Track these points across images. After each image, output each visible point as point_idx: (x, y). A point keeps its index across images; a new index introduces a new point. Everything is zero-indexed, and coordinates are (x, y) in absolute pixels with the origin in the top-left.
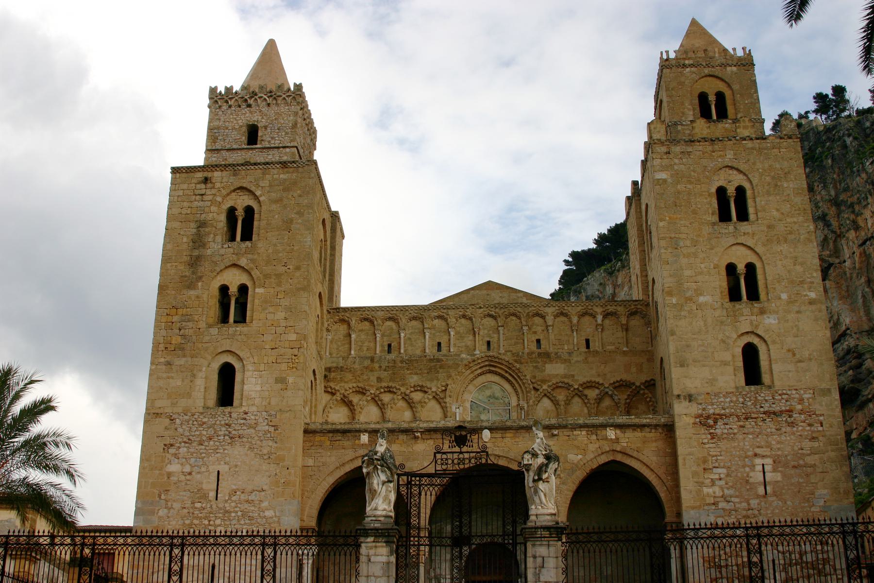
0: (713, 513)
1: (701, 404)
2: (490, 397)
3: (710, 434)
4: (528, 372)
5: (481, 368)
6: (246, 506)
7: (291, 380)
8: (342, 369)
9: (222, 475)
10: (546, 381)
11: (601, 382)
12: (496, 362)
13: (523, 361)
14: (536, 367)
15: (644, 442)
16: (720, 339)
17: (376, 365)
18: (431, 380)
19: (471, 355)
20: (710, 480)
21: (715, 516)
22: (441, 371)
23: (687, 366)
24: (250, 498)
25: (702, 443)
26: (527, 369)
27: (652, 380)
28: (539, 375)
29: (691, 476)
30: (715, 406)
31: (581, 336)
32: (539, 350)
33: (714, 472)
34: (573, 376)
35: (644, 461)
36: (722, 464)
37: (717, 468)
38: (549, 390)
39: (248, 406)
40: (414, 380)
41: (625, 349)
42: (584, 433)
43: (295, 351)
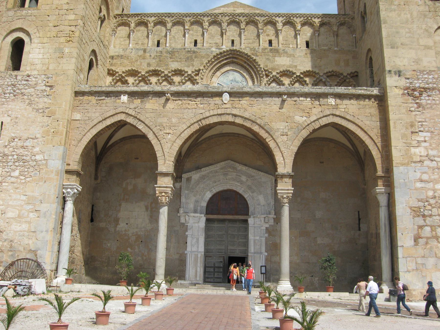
0: (419, 170)
1: (408, 79)
2: (232, 80)
3: (417, 103)
4: (262, 62)
5: (226, 59)
6: (22, 150)
7: (67, 50)
8: (121, 57)
9: (5, 125)
10: (275, 69)
11: (317, 71)
12: (238, 54)
13: (258, 54)
14: (268, 59)
15: (359, 109)
16: (424, 28)
17: (148, 55)
18: (188, 66)
19: (219, 49)
20: (417, 142)
21: (421, 172)
22: (195, 60)
23: (397, 48)
24: (25, 144)
25: (410, 110)
26: (261, 60)
27: (356, 72)
28: (270, 66)
29: (400, 138)
30: (420, 81)
31: (303, 39)
32: (271, 48)
33: (420, 135)
34: (296, 66)
35: (359, 124)
36: (426, 129)
37: (422, 132)
38: (278, 76)
39: (31, 70)
40: (174, 66)
41: (336, 49)
42: (309, 99)
43: (73, 28)
